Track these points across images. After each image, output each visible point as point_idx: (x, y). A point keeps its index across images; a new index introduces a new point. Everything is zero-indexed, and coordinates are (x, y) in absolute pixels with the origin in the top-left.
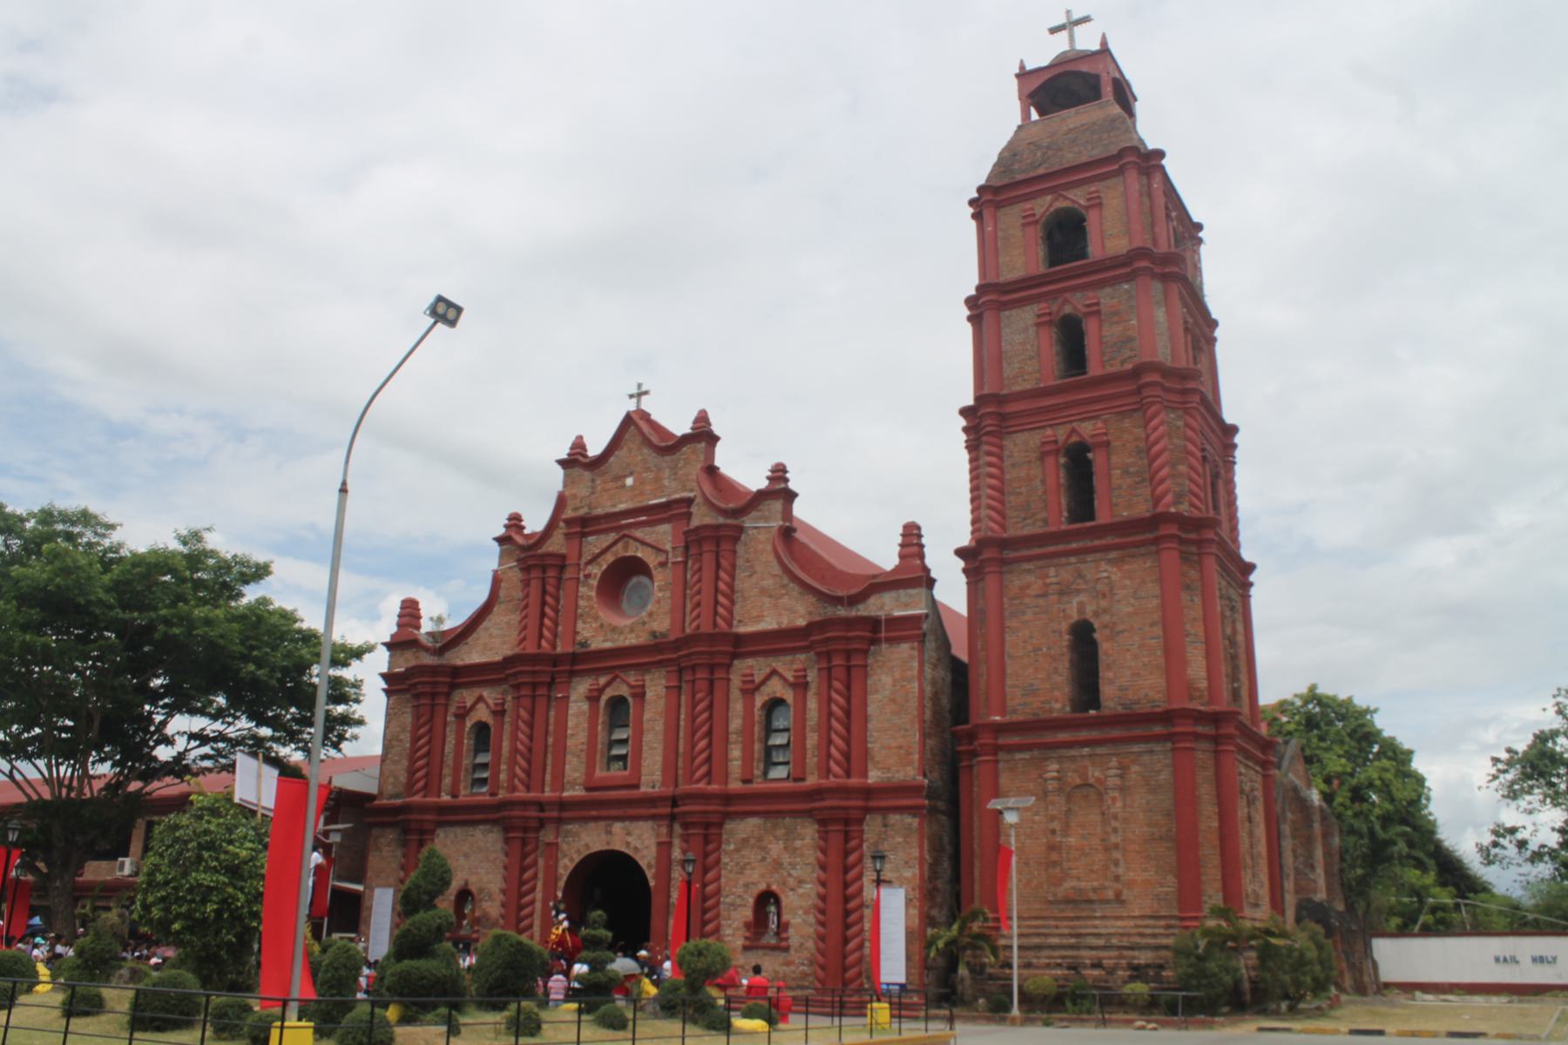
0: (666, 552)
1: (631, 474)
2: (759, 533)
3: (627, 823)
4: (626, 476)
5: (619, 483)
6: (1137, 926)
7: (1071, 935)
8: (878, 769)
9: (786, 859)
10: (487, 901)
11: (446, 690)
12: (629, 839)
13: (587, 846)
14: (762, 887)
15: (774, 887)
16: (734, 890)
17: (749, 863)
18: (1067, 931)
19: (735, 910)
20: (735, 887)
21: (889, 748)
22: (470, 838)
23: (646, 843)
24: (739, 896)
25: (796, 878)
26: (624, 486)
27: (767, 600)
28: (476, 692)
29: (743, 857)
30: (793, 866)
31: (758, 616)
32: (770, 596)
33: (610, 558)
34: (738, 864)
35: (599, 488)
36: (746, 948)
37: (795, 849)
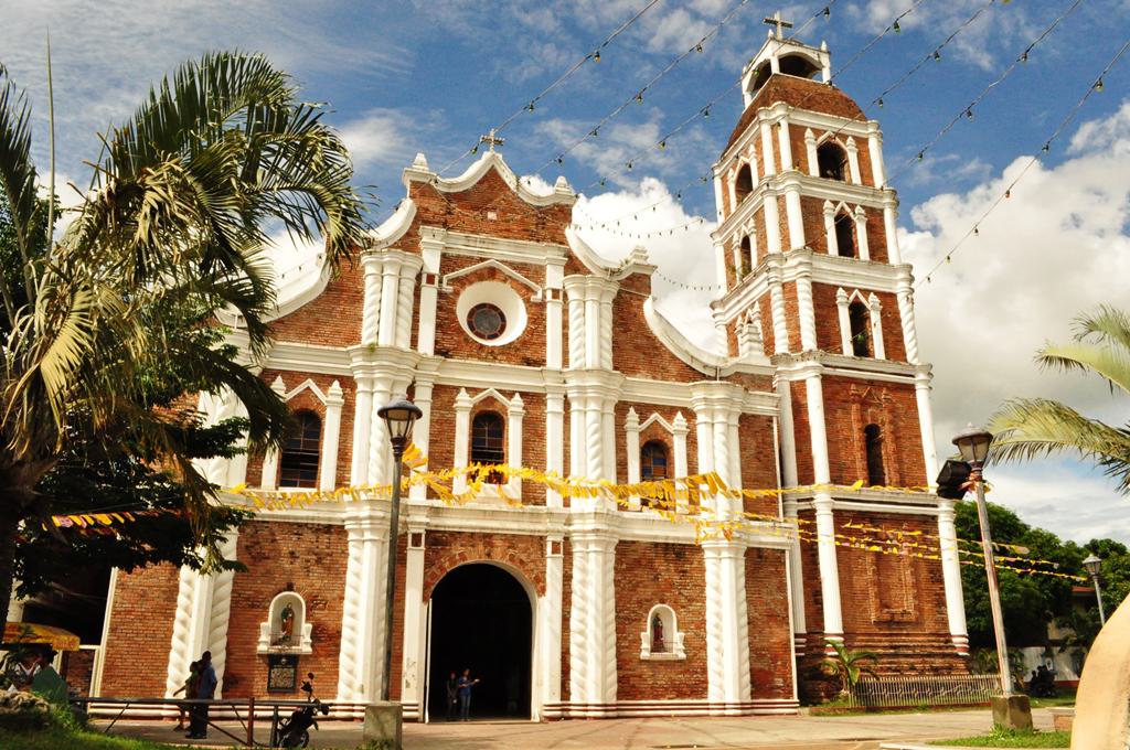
1: (494, 209)
4: (487, 209)
6: (929, 641)
7: (892, 647)
9: (676, 579)
13: (462, 556)
17: (641, 582)
18: (887, 644)
20: (629, 603)
23: (533, 557)
25: (686, 597)
27: (642, 356)
29: (636, 575)
30: (684, 586)
31: (633, 368)
32: (644, 353)
34: (630, 582)
37: (684, 572)
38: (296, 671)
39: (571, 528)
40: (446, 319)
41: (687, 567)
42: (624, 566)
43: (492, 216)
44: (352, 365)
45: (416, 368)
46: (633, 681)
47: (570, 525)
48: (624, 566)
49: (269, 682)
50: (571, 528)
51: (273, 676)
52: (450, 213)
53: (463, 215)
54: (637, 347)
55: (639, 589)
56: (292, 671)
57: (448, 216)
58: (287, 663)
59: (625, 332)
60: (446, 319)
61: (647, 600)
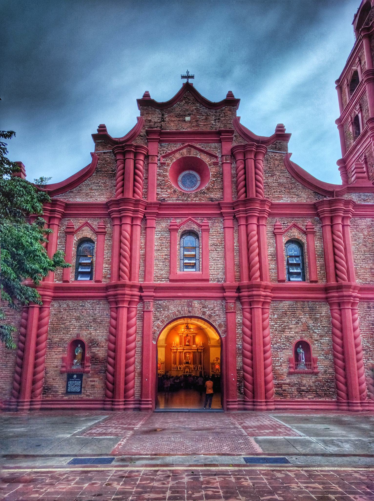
0: (216, 157)
1: (189, 115)
2: (275, 156)
3: (203, 301)
4: (185, 116)
5: (181, 119)
8: (360, 279)
10: (95, 347)
11: (60, 217)
12: (205, 310)
14: (298, 339)
15: (305, 339)
16: (279, 340)
17: (287, 326)
19: (281, 351)
21: (366, 269)
22: (80, 308)
24: (283, 344)
26: (185, 121)
27: (283, 189)
28: (82, 221)
29: (284, 322)
32: (285, 188)
33: (178, 156)
35: (167, 119)
36: (290, 374)
38: (82, 382)
39: (241, 294)
40: (164, 180)
41: (318, 316)
42: (276, 316)
43: (188, 119)
44: (109, 211)
45: (145, 209)
46: (285, 387)
47: (240, 292)
48: (276, 316)
49: (67, 388)
50: (241, 294)
51: (69, 385)
52: (163, 121)
53: (172, 121)
54: (280, 184)
55: (286, 330)
56: (80, 382)
57: (162, 123)
58: (77, 378)
59: (272, 176)
60: (164, 180)
61: (291, 337)
